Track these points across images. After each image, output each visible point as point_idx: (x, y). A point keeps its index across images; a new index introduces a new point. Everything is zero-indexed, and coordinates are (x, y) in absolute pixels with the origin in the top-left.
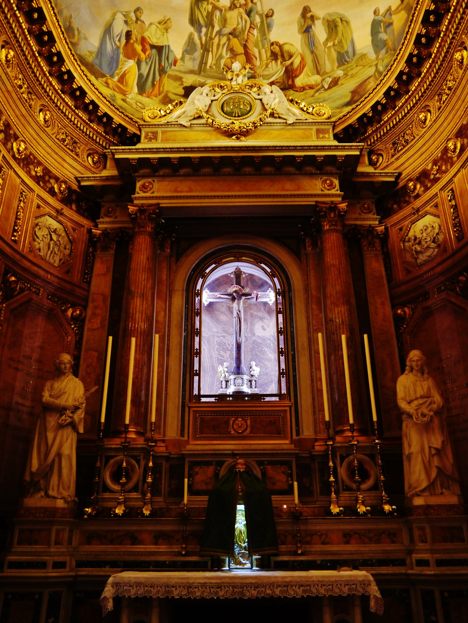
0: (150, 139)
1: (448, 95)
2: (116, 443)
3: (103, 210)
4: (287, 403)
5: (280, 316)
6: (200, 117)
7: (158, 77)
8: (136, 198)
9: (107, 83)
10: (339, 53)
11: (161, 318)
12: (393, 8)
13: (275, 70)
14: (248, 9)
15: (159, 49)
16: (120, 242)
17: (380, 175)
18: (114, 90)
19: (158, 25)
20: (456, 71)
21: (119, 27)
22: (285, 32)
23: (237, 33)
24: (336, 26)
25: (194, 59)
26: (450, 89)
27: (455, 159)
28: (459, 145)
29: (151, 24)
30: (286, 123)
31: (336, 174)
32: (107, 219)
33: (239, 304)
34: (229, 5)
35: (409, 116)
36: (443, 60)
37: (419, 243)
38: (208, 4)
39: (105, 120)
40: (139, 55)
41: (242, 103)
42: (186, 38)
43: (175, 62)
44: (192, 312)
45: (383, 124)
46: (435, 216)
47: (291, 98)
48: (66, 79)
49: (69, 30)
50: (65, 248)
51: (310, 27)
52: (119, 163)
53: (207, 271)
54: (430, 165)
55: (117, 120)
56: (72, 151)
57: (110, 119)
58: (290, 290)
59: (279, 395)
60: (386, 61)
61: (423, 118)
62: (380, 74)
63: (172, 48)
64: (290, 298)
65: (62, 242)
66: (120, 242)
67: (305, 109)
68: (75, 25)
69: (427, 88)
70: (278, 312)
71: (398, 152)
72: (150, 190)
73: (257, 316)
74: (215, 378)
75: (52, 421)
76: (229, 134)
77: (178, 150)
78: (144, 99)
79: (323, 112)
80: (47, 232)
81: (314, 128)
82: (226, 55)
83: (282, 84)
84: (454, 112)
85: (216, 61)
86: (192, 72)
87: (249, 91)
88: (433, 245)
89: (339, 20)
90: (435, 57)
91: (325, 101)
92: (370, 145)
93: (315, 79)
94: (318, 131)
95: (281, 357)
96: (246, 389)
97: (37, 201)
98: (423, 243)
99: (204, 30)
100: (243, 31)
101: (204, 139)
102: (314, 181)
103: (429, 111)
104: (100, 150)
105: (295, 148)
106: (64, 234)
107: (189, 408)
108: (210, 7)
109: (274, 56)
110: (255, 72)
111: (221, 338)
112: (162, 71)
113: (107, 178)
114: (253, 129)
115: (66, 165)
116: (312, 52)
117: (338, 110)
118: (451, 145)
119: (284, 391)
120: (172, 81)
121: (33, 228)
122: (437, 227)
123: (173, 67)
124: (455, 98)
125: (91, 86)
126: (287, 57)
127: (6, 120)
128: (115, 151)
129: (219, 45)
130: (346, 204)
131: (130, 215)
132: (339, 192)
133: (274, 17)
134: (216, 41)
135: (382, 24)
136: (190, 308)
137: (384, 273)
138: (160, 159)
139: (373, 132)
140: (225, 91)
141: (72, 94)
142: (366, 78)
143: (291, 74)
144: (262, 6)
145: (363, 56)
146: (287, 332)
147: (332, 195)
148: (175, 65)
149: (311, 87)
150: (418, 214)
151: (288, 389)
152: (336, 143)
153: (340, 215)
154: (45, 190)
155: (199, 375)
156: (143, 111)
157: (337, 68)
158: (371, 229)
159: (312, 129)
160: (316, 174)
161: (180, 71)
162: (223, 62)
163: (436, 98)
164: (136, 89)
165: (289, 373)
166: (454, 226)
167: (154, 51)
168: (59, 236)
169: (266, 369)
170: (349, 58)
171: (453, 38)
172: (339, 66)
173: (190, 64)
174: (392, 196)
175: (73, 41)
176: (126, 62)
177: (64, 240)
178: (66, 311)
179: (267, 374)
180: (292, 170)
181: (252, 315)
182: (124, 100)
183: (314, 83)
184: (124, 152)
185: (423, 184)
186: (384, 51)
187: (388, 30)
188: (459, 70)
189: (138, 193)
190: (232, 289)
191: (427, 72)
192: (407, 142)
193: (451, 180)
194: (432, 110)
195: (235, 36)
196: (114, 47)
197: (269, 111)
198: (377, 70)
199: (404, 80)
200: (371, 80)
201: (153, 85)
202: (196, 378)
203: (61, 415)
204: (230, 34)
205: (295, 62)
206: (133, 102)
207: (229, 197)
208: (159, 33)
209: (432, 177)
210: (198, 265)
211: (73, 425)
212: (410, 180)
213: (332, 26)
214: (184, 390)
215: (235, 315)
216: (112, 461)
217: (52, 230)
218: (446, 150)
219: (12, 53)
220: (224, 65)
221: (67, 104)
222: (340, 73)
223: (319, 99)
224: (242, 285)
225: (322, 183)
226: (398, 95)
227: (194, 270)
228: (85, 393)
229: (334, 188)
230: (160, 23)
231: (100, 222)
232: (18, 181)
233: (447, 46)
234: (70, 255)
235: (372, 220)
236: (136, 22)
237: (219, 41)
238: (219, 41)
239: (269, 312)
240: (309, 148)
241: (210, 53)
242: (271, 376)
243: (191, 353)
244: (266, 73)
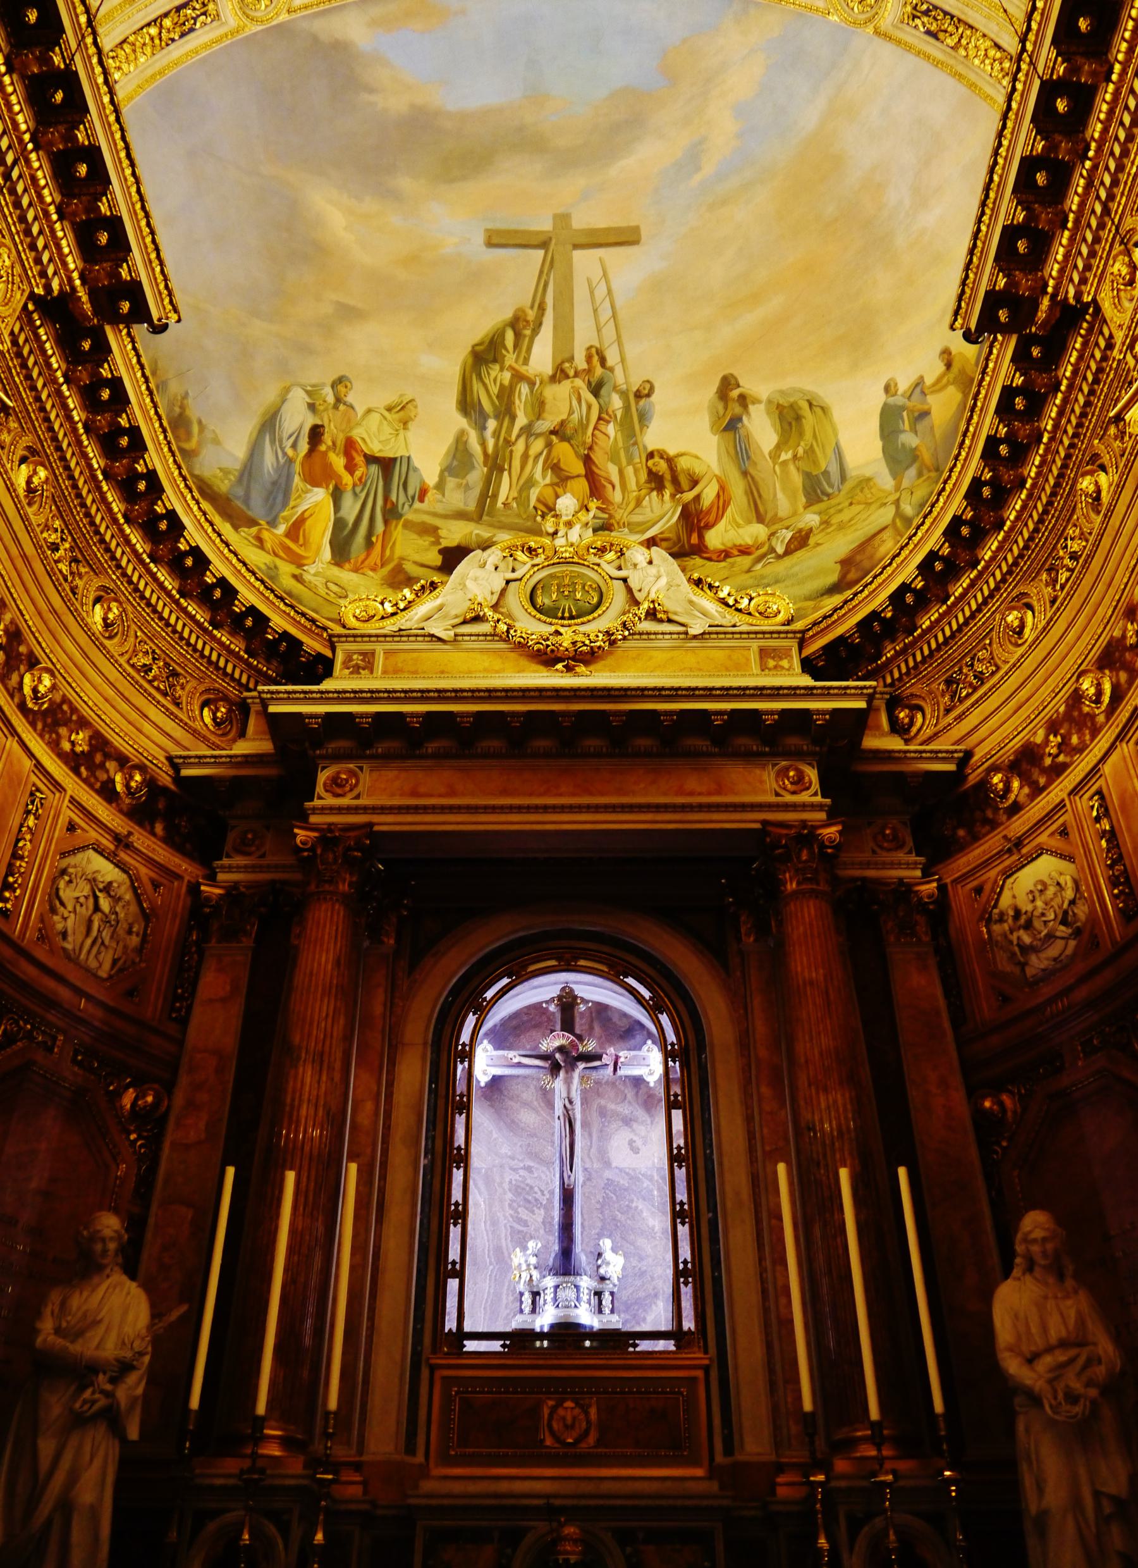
0: (357, 670)
1: (1072, 570)
2: (225, 1471)
3: (231, 837)
4: (697, 1356)
5: (677, 1116)
6: (477, 619)
7: (380, 527)
8: (314, 810)
9: (259, 539)
10: (807, 475)
11: (364, 1120)
12: (929, 381)
13: (658, 512)
14: (594, 381)
15: (387, 465)
16: (271, 918)
17: (920, 756)
18: (276, 555)
19: (386, 414)
20: (1087, 517)
21: (296, 417)
22: (681, 428)
23: (569, 432)
24: (798, 418)
25: (467, 488)
26: (1074, 556)
27: (1101, 719)
28: (1107, 687)
29: (369, 411)
30: (686, 633)
31: (812, 754)
32: (239, 860)
33: (568, 1082)
34: (550, 373)
35: (981, 619)
36: (1054, 494)
37: (1028, 926)
38: (502, 369)
39: (249, 622)
40: (340, 478)
41: (578, 587)
42: (449, 440)
43: (423, 494)
44: (447, 1101)
45: (921, 636)
46: (1062, 857)
47: (696, 576)
48: (164, 532)
49: (178, 425)
50: (130, 932)
51: (740, 419)
52: (277, 725)
53: (489, 995)
54: (1041, 733)
55: (279, 622)
56: (165, 694)
57: (262, 620)
58: (701, 1046)
59: (676, 1334)
60: (920, 494)
61: (1016, 623)
62: (908, 521)
63: (416, 462)
64: (703, 1068)
65: (122, 915)
66: (271, 918)
67: (731, 601)
68: (193, 413)
69: (1021, 556)
70: (671, 1105)
71: (961, 701)
72: (351, 790)
73: (616, 1114)
74: (503, 1288)
75: (55, 1404)
76: (547, 658)
77: (424, 696)
78: (346, 576)
79: (775, 608)
80: (87, 890)
81: (755, 645)
82: (543, 479)
83: (675, 545)
84: (1088, 610)
85: (520, 491)
86: (461, 515)
87: (597, 560)
88: (1062, 930)
89: (805, 406)
90: (1034, 485)
91: (777, 582)
92: (892, 685)
94: (764, 653)
95: (680, 1227)
96: (586, 1317)
97: (68, 814)
98: (1037, 924)
99: (492, 424)
100: (583, 426)
101: (486, 670)
102: (758, 771)
103: (1029, 607)
104: (233, 692)
105: (709, 693)
106: (128, 896)
107: (433, 1369)
108: (507, 376)
109: (656, 481)
110: (611, 516)
111: (522, 1172)
112: (391, 513)
113: (247, 760)
114: (606, 646)
115: (147, 728)
116: (745, 473)
117: (811, 604)
118: (1087, 685)
119: (688, 1324)
120: (415, 536)
121: (54, 880)
122: (1070, 884)
123: (417, 505)
124: (1088, 579)
125: (222, 546)
126: (684, 483)
127: (12, 622)
128: (269, 696)
129: (525, 457)
130: (839, 828)
131: (298, 850)
132: (819, 799)
133: (654, 398)
134: (520, 447)
135: (905, 414)
136: (442, 1092)
137: (942, 1003)
138: (378, 715)
139: (897, 654)
140: (540, 560)
141: (175, 564)
142: (873, 532)
143: (694, 521)
144: (627, 374)
145: (865, 483)
146: (693, 1158)
147: (804, 807)
148: (422, 500)
149: (744, 551)
150: (1019, 852)
151: (700, 1317)
152: (807, 681)
153: (823, 855)
154: (91, 786)
155: (460, 1275)
156: (342, 602)
157: (805, 508)
158: (904, 889)
159: (748, 648)
160: (759, 754)
161: (435, 515)
162: (534, 494)
163: (1044, 576)
164: (327, 554)
165: (701, 1274)
166: (1113, 882)
167: (374, 469)
168: (117, 899)
169: (641, 1259)
170: (831, 486)
171: (1072, 446)
172: (809, 504)
173: (457, 498)
174: (953, 808)
175: (186, 446)
176: (307, 492)
177: (127, 912)
178: (119, 1094)
179: (642, 1274)
180: (702, 744)
181: (603, 1112)
182: (295, 577)
183: (750, 542)
184: (290, 698)
185: (1026, 779)
186: (912, 472)
187: (919, 427)
188: (1093, 515)
189: (320, 798)
190: (552, 1042)
191: (1017, 518)
192: (980, 676)
193: (1095, 771)
194: (1035, 603)
195: (564, 438)
196: (282, 461)
197: (645, 606)
198: (899, 513)
199: (964, 538)
200: (886, 535)
201: (369, 544)
202: (453, 1284)
203: (82, 1388)
204: (553, 432)
205: (704, 495)
206: (318, 582)
207: (545, 809)
208: (387, 430)
209: (1048, 761)
210: (465, 980)
211: (112, 1418)
212: (995, 769)
213: (789, 418)
214: (419, 1318)
215: (559, 1110)
216: (212, 1526)
217: (101, 886)
218: (1077, 697)
219: (42, 473)
220: (538, 500)
221: (161, 585)
222: (811, 519)
223: (763, 577)
224: (578, 1031)
225: (778, 775)
226: (953, 570)
227: (456, 991)
228: (150, 1327)
229: (808, 788)
230: (389, 409)
231: (222, 867)
232: (28, 764)
233: (1059, 463)
234: (140, 950)
235: (905, 868)
236: (336, 407)
237: (527, 447)
238: (527, 447)
239: (648, 1103)
240: (743, 693)
241: (506, 473)
242: (652, 1278)
243: (442, 1213)
244: (636, 518)
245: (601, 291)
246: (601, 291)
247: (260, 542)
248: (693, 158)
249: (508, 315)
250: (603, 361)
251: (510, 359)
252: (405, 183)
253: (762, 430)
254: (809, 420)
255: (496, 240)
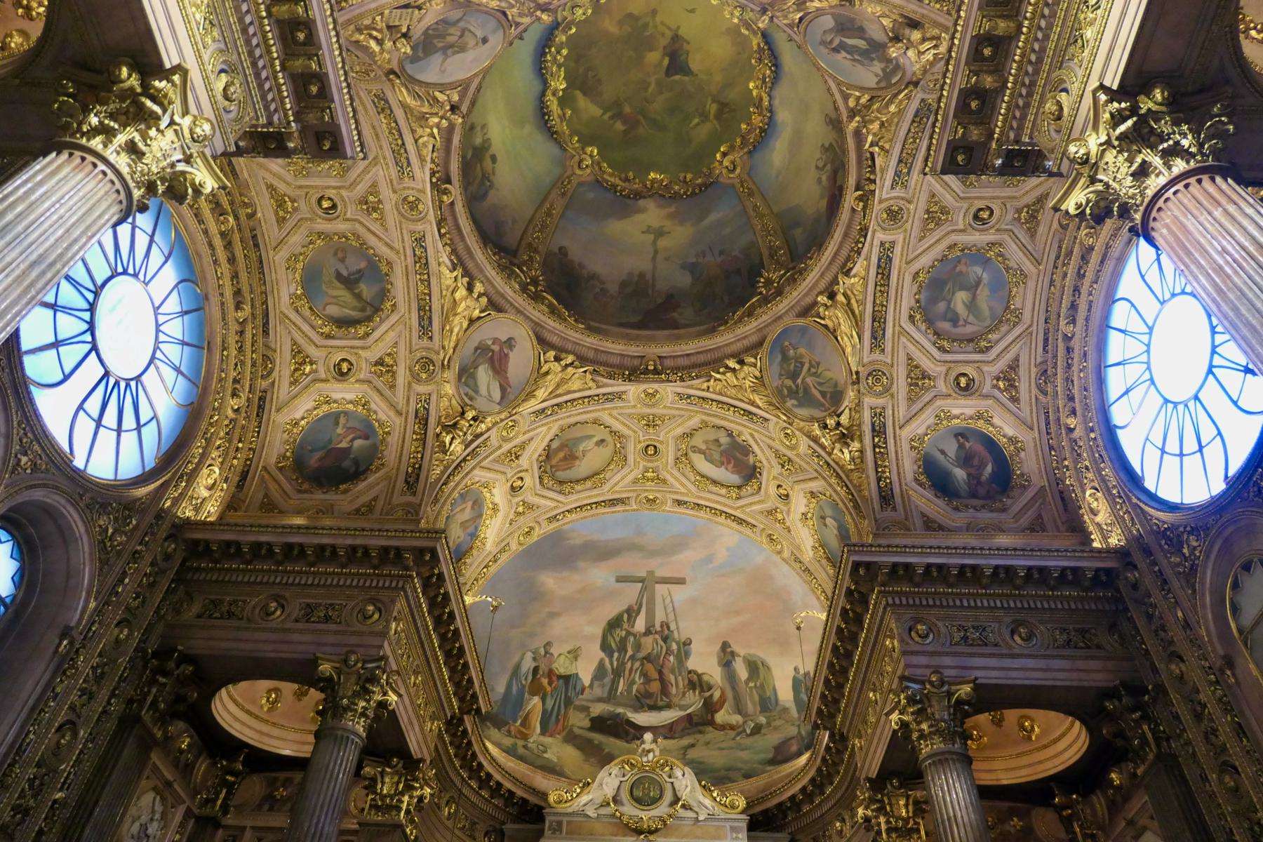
7: (563, 711)
9: (509, 731)
10: (761, 697)
13: (693, 700)
15: (566, 679)
21: (528, 664)
22: (704, 662)
24: (757, 668)
25: (603, 686)
34: (643, 631)
63: (581, 676)
78: (547, 740)
81: (728, 825)
82: (639, 680)
86: (600, 700)
93: (736, 719)
99: (616, 655)
100: (658, 656)
104: (497, 826)
108: (624, 633)
112: (568, 702)
116: (733, 688)
129: (631, 670)
134: (629, 664)
139: (793, 820)
143: (710, 707)
145: (786, 710)
149: (732, 728)
162: (635, 688)
164: (538, 730)
167: (561, 681)
172: (761, 712)
173: (598, 692)
182: (525, 747)
195: (649, 661)
198: (799, 732)
200: (794, 741)
201: (557, 720)
206: (533, 746)
208: (568, 662)
222: (762, 720)
244: (682, 703)
245: (668, 600)
246: (668, 600)
247: (509, 733)
248: (709, 559)
249: (625, 607)
250: (668, 628)
251: (625, 626)
252: (581, 564)
253: (742, 673)
254: (762, 671)
255: (620, 580)
